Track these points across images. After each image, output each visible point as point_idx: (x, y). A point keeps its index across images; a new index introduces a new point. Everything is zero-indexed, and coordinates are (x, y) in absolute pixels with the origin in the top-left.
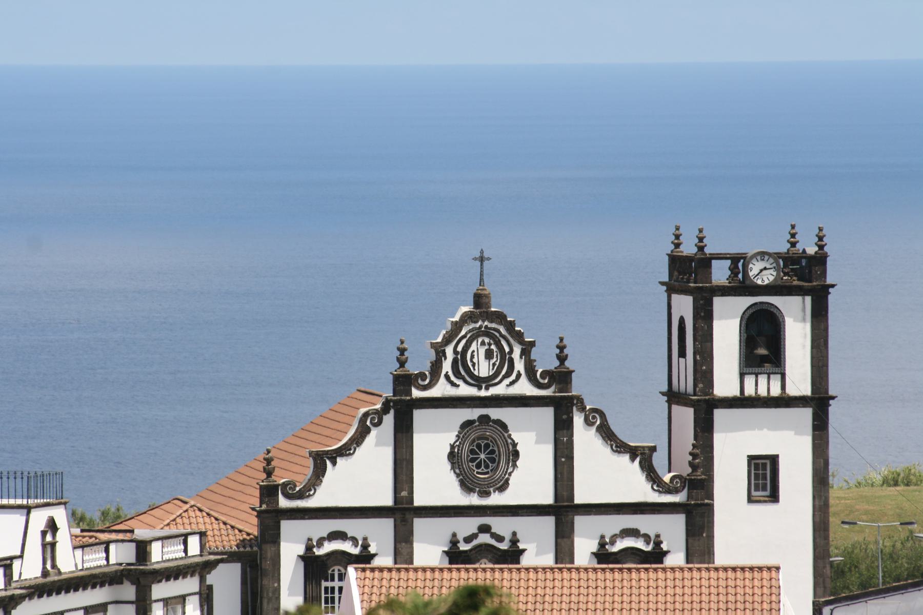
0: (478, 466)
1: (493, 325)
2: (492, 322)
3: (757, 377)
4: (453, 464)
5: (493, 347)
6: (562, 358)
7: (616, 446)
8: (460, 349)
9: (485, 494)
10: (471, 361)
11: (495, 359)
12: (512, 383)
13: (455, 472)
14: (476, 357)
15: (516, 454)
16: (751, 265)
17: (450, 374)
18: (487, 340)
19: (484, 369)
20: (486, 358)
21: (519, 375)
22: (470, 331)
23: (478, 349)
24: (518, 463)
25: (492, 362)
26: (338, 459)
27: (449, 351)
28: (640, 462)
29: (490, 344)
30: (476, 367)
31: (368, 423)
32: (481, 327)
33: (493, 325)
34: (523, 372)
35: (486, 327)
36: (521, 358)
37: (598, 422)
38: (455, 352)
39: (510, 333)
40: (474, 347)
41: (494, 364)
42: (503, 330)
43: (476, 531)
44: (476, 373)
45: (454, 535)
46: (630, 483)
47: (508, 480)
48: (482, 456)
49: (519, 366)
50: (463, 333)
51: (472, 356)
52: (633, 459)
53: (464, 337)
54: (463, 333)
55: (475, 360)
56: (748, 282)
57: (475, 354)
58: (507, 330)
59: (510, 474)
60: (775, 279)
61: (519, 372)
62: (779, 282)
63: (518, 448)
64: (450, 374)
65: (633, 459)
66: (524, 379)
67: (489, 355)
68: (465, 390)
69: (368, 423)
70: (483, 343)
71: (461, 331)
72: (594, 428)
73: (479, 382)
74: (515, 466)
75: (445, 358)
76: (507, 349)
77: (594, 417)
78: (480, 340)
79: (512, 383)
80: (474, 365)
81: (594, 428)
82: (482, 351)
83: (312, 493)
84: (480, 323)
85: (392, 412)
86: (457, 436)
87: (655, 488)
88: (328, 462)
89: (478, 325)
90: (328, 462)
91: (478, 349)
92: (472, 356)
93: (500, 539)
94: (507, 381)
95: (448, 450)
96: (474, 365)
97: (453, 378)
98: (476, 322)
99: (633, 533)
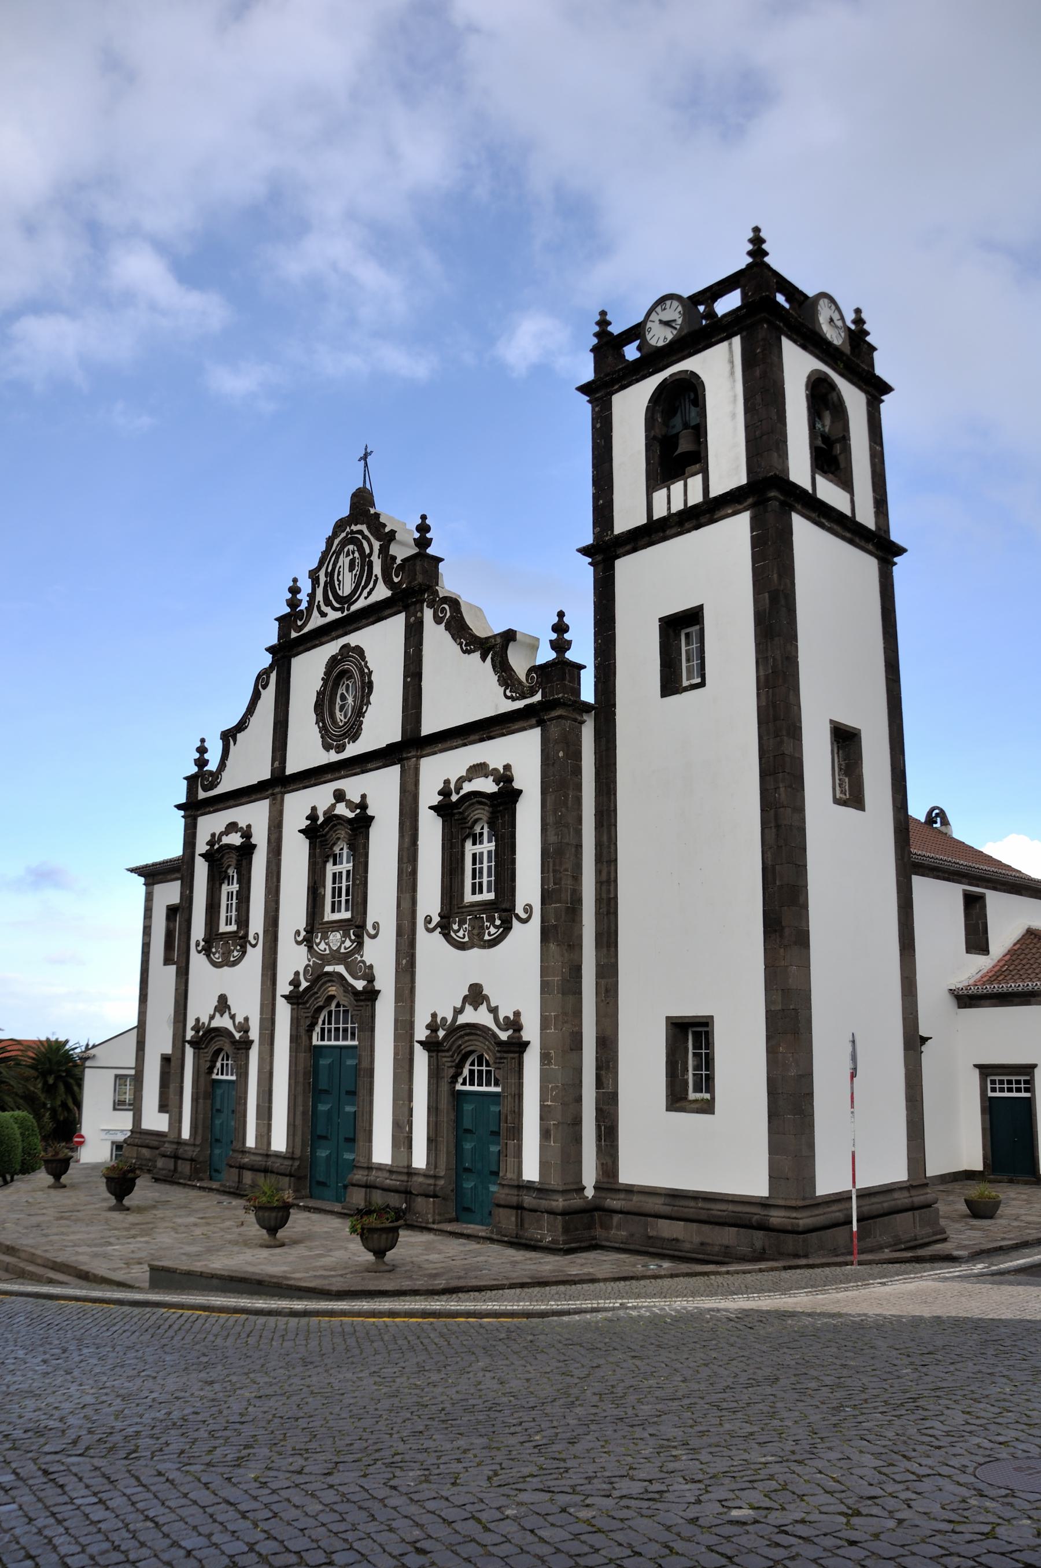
3: (669, 489)
6: (423, 542)
9: (340, 749)
10: (338, 580)
12: (369, 593)
29: (353, 553)
42: (363, 528)
45: (314, 809)
55: (341, 578)
64: (322, 604)
68: (333, 615)
76: (367, 551)
79: (369, 593)
82: (347, 560)
84: (348, 529)
87: (508, 694)
97: (324, 608)
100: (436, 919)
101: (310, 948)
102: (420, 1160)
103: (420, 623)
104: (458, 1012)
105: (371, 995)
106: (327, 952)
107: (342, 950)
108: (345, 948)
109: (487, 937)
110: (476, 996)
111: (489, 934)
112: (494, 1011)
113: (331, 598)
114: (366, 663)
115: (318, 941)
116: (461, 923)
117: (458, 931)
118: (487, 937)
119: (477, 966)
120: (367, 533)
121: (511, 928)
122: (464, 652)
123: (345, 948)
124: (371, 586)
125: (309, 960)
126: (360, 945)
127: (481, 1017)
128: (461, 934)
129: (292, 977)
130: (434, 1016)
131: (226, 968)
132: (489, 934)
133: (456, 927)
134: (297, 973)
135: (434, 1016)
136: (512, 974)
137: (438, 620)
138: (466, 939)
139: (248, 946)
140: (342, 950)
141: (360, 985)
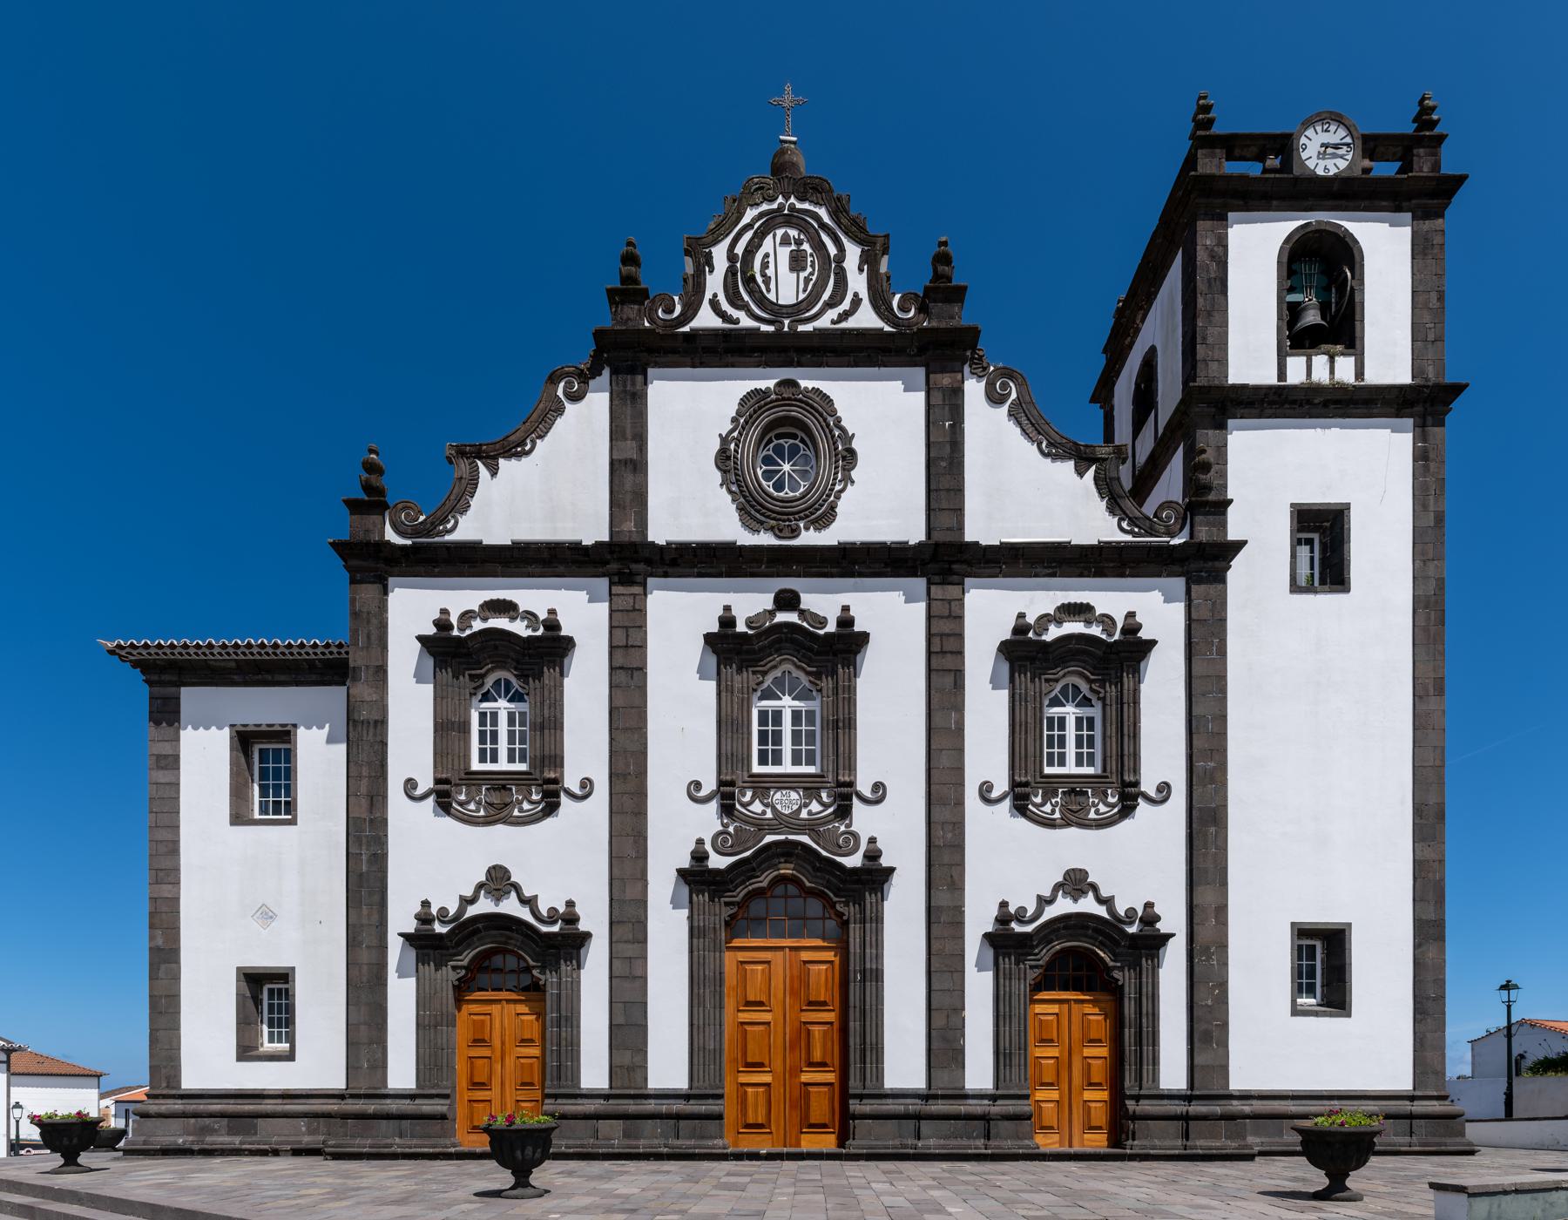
0: (779, 486)
1: (806, 206)
2: (801, 199)
4: (724, 472)
5: (806, 246)
7: (1050, 444)
8: (739, 249)
10: (764, 275)
11: (809, 269)
12: (845, 316)
13: (730, 491)
14: (772, 265)
15: (850, 457)
16: (1303, 140)
17: (722, 298)
18: (793, 233)
19: (787, 289)
20: (792, 269)
21: (857, 302)
22: (761, 215)
23: (776, 252)
24: (853, 474)
25: (803, 275)
26: (501, 461)
27: (719, 253)
28: (1096, 479)
29: (799, 242)
30: (773, 286)
31: (560, 393)
32: (781, 207)
33: (806, 206)
34: (864, 294)
35: (792, 208)
36: (861, 270)
37: (1014, 395)
38: (732, 257)
39: (838, 223)
40: (768, 245)
41: (807, 280)
42: (823, 212)
43: (770, 606)
44: (772, 296)
46: (1071, 507)
47: (833, 508)
48: (786, 467)
49: (858, 283)
50: (746, 220)
51: (765, 265)
52: (1080, 473)
53: (749, 226)
54: (746, 220)
55: (770, 272)
56: (1297, 171)
57: (771, 259)
58: (833, 214)
59: (838, 497)
60: (1349, 167)
61: (856, 295)
62: (1357, 173)
63: (854, 445)
64: (722, 298)
65: (1080, 473)
66: (866, 304)
67: (797, 262)
69: (560, 393)
70: (785, 241)
71: (741, 216)
72: (1006, 407)
73: (776, 312)
74: (848, 480)
75: (711, 271)
76: (833, 250)
77: (1004, 386)
78: (780, 232)
79: (845, 316)
80: (767, 280)
81: (1006, 407)
82: (784, 253)
83: (449, 526)
84: (780, 199)
85: (606, 372)
86: (734, 420)
87: (1124, 525)
88: (483, 471)
89: (775, 206)
90: (483, 471)
91: (776, 252)
92: (765, 265)
93: (823, 622)
94: (833, 314)
95: (716, 445)
96: (767, 280)
98: (773, 200)
99: (1080, 611)
100: (1001, 786)
101: (727, 810)
102: (979, 1073)
103: (957, 393)
104: (1043, 902)
105: (875, 877)
106: (769, 815)
107: (804, 814)
108: (810, 813)
109: (1092, 815)
110: (1076, 883)
111: (1097, 812)
112: (1107, 902)
113: (746, 297)
114: (839, 420)
115: (747, 798)
116: (1049, 794)
117: (1043, 804)
118: (1092, 815)
119: (1074, 847)
120: (826, 219)
121: (1134, 807)
122: (1045, 455)
123: (810, 813)
124: (846, 305)
125: (725, 826)
126: (844, 812)
127: (1088, 905)
128: (1048, 808)
129: (692, 846)
130: (1004, 905)
131: (500, 827)
132: (1097, 812)
133: (1038, 800)
134: (700, 842)
135: (1004, 905)
136: (1138, 864)
137: (995, 399)
138: (1057, 815)
139: (564, 798)
140: (804, 814)
141: (854, 861)
